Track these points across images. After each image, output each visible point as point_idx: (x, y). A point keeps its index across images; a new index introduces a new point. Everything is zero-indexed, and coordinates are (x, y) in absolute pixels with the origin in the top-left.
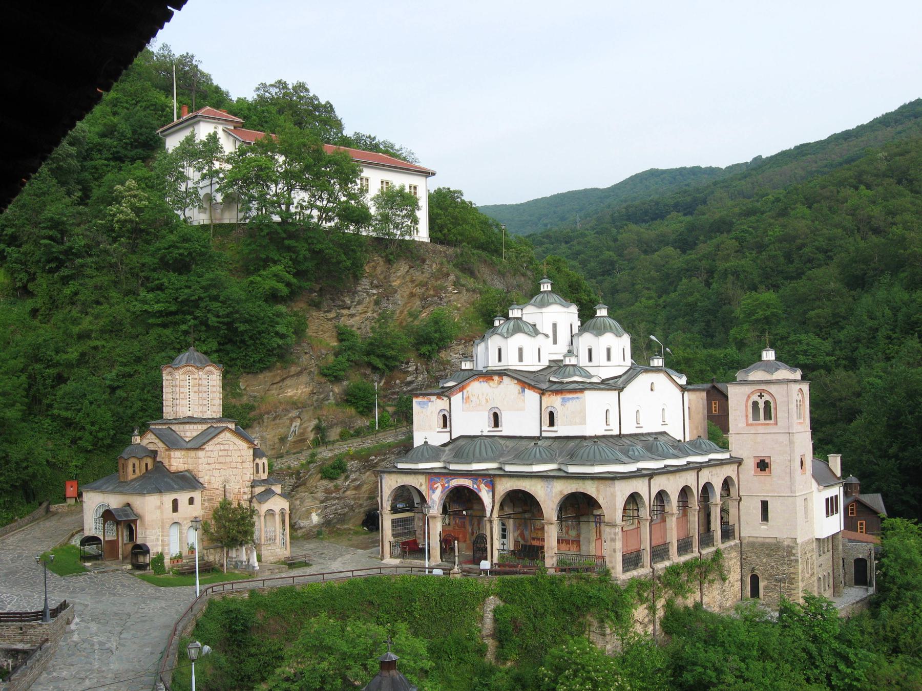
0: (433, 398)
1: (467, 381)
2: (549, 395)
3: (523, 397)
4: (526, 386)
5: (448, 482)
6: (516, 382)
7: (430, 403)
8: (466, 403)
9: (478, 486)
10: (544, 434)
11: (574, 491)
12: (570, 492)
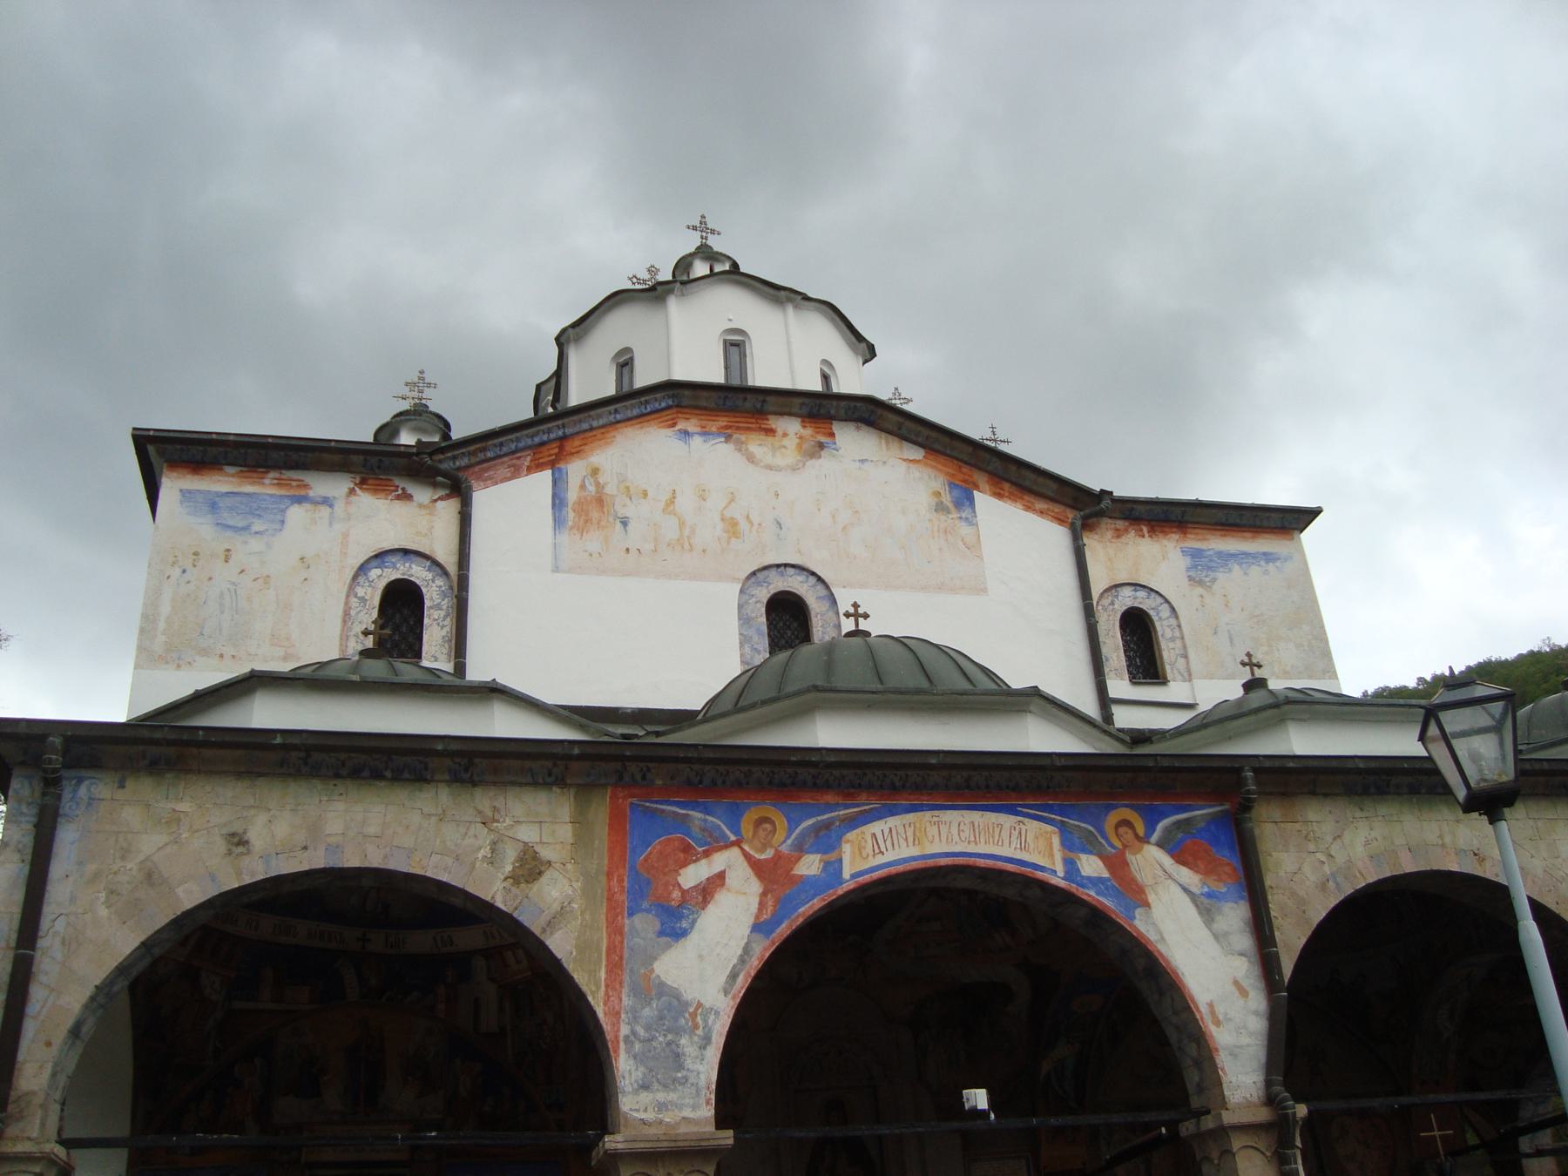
0: (333, 486)
1: (605, 417)
2: (1119, 534)
3: (965, 530)
4: (981, 479)
5: (825, 840)
6: (917, 453)
7: (296, 513)
9: (1117, 865)
10: (1124, 718)
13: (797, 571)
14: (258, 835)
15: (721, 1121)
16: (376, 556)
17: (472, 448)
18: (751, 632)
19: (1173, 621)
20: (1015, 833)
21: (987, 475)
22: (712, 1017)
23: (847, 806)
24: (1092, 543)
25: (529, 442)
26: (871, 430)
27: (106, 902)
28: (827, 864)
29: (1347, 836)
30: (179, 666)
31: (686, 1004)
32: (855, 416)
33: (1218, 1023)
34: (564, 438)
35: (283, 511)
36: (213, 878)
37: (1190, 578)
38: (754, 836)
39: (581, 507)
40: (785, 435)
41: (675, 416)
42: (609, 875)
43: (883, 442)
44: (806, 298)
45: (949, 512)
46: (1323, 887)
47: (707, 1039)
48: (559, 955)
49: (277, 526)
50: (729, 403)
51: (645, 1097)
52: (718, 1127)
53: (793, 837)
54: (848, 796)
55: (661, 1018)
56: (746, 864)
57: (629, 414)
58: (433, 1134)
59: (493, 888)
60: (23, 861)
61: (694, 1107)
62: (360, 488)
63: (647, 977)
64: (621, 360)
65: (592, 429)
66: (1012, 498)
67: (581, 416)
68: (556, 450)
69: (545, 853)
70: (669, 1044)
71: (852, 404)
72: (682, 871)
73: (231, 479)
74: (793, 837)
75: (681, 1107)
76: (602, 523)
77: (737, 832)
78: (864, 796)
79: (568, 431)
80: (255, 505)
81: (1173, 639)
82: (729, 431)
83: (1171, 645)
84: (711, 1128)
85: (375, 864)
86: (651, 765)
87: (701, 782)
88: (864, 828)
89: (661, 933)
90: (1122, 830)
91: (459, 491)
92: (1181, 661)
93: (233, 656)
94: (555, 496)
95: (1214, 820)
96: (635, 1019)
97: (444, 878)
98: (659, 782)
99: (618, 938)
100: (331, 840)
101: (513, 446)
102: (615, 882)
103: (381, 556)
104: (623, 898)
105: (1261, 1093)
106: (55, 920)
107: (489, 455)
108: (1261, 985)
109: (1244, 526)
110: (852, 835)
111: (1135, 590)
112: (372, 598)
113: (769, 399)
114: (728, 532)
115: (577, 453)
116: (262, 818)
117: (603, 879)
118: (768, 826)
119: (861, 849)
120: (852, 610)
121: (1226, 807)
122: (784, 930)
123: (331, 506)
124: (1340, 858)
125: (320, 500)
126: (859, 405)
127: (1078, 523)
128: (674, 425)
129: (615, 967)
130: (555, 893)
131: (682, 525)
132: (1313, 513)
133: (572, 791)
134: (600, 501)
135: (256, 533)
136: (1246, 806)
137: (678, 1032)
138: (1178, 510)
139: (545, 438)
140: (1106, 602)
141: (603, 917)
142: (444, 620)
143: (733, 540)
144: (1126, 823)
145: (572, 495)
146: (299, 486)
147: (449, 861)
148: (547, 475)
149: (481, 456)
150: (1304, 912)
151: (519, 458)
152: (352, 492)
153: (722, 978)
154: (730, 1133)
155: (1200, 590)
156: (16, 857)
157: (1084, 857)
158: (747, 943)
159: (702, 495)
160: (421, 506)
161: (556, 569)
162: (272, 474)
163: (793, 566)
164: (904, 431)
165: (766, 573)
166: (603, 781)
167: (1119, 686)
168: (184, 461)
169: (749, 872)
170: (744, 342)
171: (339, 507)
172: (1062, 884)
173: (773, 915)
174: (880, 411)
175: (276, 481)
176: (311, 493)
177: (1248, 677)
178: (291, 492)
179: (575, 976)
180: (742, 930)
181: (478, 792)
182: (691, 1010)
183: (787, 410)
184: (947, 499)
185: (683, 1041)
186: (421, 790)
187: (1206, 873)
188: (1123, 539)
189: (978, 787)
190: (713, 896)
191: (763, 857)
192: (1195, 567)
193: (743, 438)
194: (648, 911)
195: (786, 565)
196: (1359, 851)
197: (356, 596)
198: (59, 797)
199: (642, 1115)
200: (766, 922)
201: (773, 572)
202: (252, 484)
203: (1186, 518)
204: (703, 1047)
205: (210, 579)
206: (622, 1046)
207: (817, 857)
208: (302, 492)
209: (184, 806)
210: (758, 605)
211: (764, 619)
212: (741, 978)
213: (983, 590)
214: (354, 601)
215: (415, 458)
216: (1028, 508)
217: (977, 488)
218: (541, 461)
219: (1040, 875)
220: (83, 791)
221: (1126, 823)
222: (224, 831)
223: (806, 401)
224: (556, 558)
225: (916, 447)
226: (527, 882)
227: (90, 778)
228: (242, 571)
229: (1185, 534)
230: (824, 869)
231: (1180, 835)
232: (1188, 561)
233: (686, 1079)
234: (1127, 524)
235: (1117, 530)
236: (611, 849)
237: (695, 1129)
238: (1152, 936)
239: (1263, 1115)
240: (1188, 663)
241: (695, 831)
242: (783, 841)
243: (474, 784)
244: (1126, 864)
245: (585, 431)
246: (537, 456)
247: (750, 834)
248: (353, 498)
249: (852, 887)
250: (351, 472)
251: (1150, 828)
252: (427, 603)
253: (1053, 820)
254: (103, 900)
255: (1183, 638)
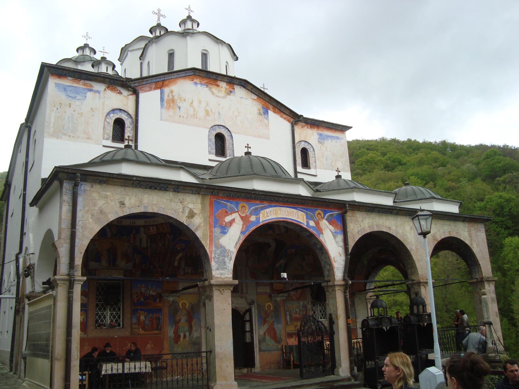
2: (303, 127)
3: (266, 121)
4: (271, 107)
5: (256, 212)
6: (255, 97)
7: (89, 94)
8: (169, 108)
9: (317, 223)
10: (300, 176)
11: (447, 235)
12: (443, 237)
13: (223, 127)
14: (127, 202)
15: (235, 277)
16: (112, 110)
17: (140, 81)
18: (211, 143)
19: (313, 152)
20: (297, 214)
21: (272, 106)
22: (232, 253)
23: (261, 205)
24: (297, 129)
25: (155, 81)
26: (244, 89)
27: (91, 218)
28: (257, 218)
29: (364, 222)
30: (57, 138)
31: (226, 250)
32: (241, 84)
33: (335, 262)
34: (164, 80)
35: (86, 93)
36: (117, 213)
37: (319, 141)
38: (241, 210)
39: (168, 100)
40: (222, 87)
41: (193, 77)
42: (209, 217)
43: (247, 92)
44: (225, 43)
45: (262, 115)
46: (358, 233)
47: (231, 259)
48: (198, 236)
49: (84, 98)
50: (208, 76)
51: (218, 272)
52: (233, 279)
53: (250, 211)
54: (262, 202)
55: (221, 253)
56: (239, 217)
57: (182, 75)
58: (168, 278)
59: (183, 219)
60: (69, 206)
61: (228, 274)
62: (108, 89)
63: (218, 243)
64: (170, 52)
65: (172, 79)
66: (278, 113)
67: (170, 75)
68: (162, 84)
69: (195, 211)
70: (223, 259)
71: (240, 81)
72: (226, 218)
73: (70, 81)
74: (250, 211)
75: (225, 274)
76: (174, 108)
77: (237, 208)
78: (265, 202)
79: (165, 79)
80: (77, 90)
81: (313, 157)
82: (207, 84)
83: (312, 159)
84: (232, 280)
85: (156, 212)
86: (220, 191)
87: (230, 196)
88: (264, 210)
89: (221, 233)
90: (319, 215)
91: (136, 93)
92: (315, 163)
93: (73, 137)
94: (161, 98)
95: (338, 215)
96: (215, 253)
97: (172, 216)
98: (221, 195)
99: (212, 233)
100: (144, 205)
101: (150, 81)
102: (211, 219)
103: (114, 110)
104: (212, 223)
105: (342, 278)
106: (79, 222)
107: (144, 83)
108: (344, 254)
109: (333, 129)
110: (262, 212)
111: (305, 143)
112: (111, 122)
113: (220, 76)
114: (206, 114)
115: (167, 85)
116: (128, 198)
117: (208, 218)
118: (244, 208)
119: (264, 215)
120: (247, 146)
121: (341, 212)
122: (247, 233)
123: (99, 93)
124: (362, 226)
125: (96, 91)
126: (242, 81)
127: (294, 123)
128: (193, 80)
129: (211, 240)
130: (197, 221)
131: (194, 110)
132: (350, 128)
133: (201, 195)
134: (173, 101)
135: (78, 99)
136: (346, 212)
137: (224, 256)
138: (318, 122)
139: (159, 80)
140: (298, 145)
141: (208, 228)
142: (131, 131)
143: (207, 116)
144: (320, 214)
145: (166, 98)
146: (90, 86)
147: (173, 212)
148: (158, 91)
149: (142, 83)
150: (354, 238)
151: (151, 85)
152: (105, 90)
153: (234, 244)
154: (237, 281)
155: (320, 145)
156: (67, 204)
157: (310, 221)
158: (240, 236)
159: (200, 102)
160: (125, 96)
161: (161, 120)
162: (82, 81)
163: (222, 126)
164: (253, 90)
165: (215, 127)
166: (208, 194)
167: (299, 169)
168: (56, 74)
169: (240, 219)
170: (207, 54)
171: (102, 94)
172: (306, 227)
173: (245, 230)
174: (247, 84)
175: (83, 84)
176: (94, 89)
177: (337, 174)
178: (88, 88)
179: (202, 242)
180: (238, 233)
181: (179, 194)
182: (228, 251)
183: (223, 80)
184: (262, 112)
185: (226, 259)
186: (166, 193)
187: (335, 227)
188: (303, 128)
189: (290, 202)
190: (232, 224)
191: (243, 215)
192: (320, 138)
193: (211, 86)
194: (218, 227)
195: (220, 125)
196: (366, 225)
197: (107, 122)
198: (77, 189)
199: (217, 276)
200: (244, 231)
201: (217, 127)
202: (76, 83)
203: (320, 125)
204: (230, 260)
205: (65, 112)
206: (213, 259)
207: (255, 216)
208: (91, 88)
209: (108, 194)
210: (213, 136)
211: (214, 140)
212: (238, 245)
213: (269, 139)
214: (106, 123)
215: (125, 82)
216: (281, 117)
217: (269, 109)
218: (158, 87)
219: (301, 224)
220: (82, 187)
221: (320, 214)
222: (119, 201)
223: (229, 78)
224: (161, 116)
225: (255, 95)
226: (191, 218)
227: (83, 184)
228: (75, 111)
229: (318, 129)
230: (256, 220)
231: (330, 218)
232: (318, 137)
233: (226, 267)
234: (305, 124)
235: (302, 126)
236: (210, 211)
237: (228, 279)
238: (323, 241)
239: (343, 283)
240: (316, 164)
241: (229, 208)
242: (247, 212)
243: (178, 192)
244: (319, 223)
245: (170, 79)
246: (156, 85)
247: (240, 210)
248: (106, 92)
249: (262, 224)
250: (105, 84)
251: (325, 216)
252: (126, 126)
253: (305, 212)
254: (90, 217)
255: (315, 157)
